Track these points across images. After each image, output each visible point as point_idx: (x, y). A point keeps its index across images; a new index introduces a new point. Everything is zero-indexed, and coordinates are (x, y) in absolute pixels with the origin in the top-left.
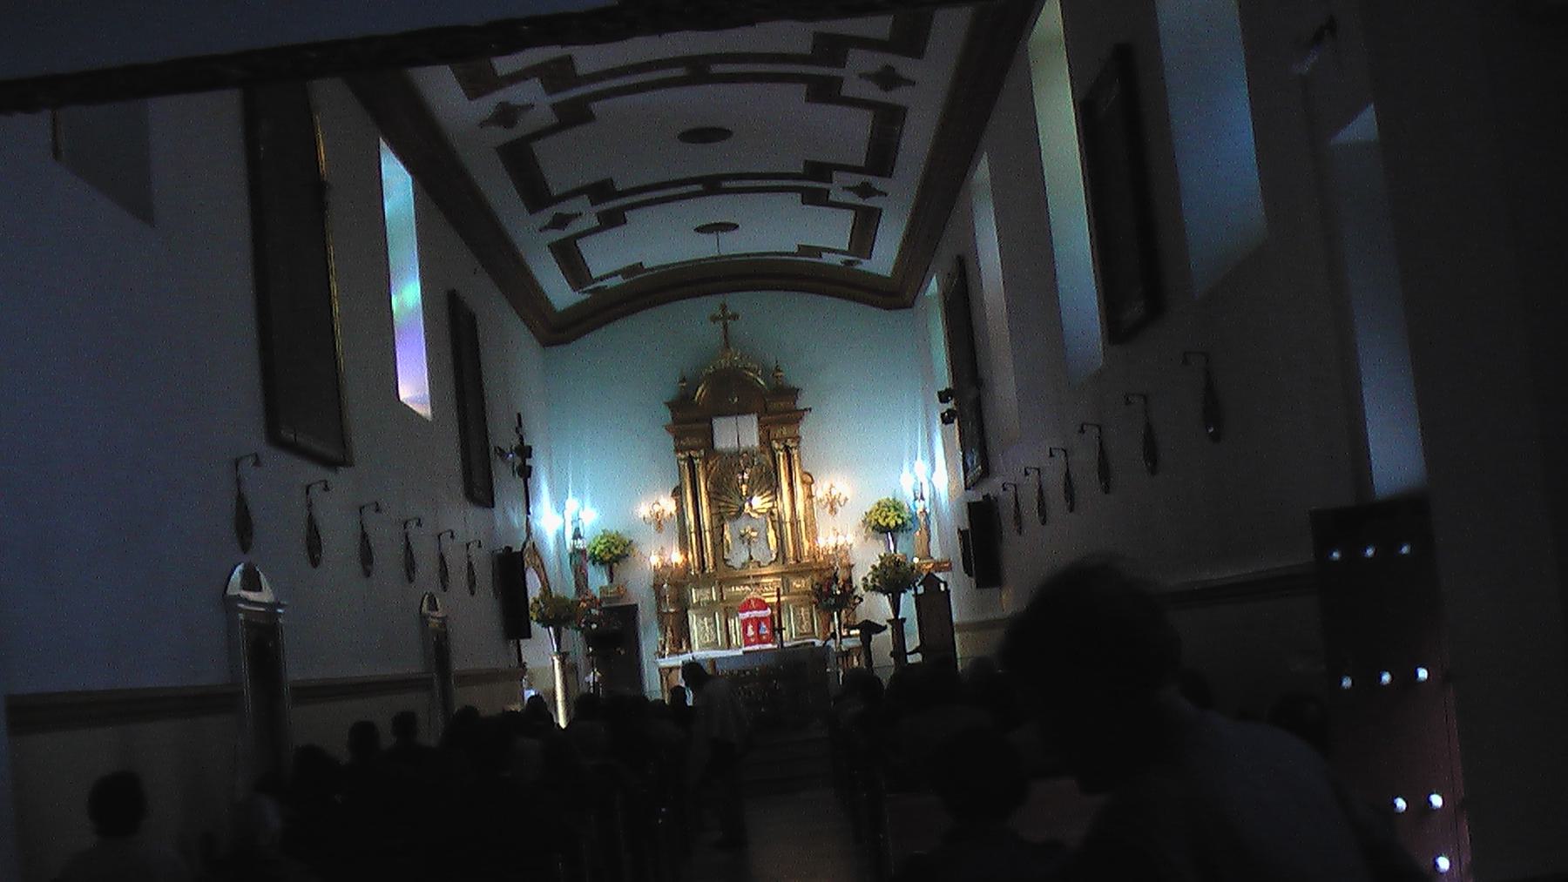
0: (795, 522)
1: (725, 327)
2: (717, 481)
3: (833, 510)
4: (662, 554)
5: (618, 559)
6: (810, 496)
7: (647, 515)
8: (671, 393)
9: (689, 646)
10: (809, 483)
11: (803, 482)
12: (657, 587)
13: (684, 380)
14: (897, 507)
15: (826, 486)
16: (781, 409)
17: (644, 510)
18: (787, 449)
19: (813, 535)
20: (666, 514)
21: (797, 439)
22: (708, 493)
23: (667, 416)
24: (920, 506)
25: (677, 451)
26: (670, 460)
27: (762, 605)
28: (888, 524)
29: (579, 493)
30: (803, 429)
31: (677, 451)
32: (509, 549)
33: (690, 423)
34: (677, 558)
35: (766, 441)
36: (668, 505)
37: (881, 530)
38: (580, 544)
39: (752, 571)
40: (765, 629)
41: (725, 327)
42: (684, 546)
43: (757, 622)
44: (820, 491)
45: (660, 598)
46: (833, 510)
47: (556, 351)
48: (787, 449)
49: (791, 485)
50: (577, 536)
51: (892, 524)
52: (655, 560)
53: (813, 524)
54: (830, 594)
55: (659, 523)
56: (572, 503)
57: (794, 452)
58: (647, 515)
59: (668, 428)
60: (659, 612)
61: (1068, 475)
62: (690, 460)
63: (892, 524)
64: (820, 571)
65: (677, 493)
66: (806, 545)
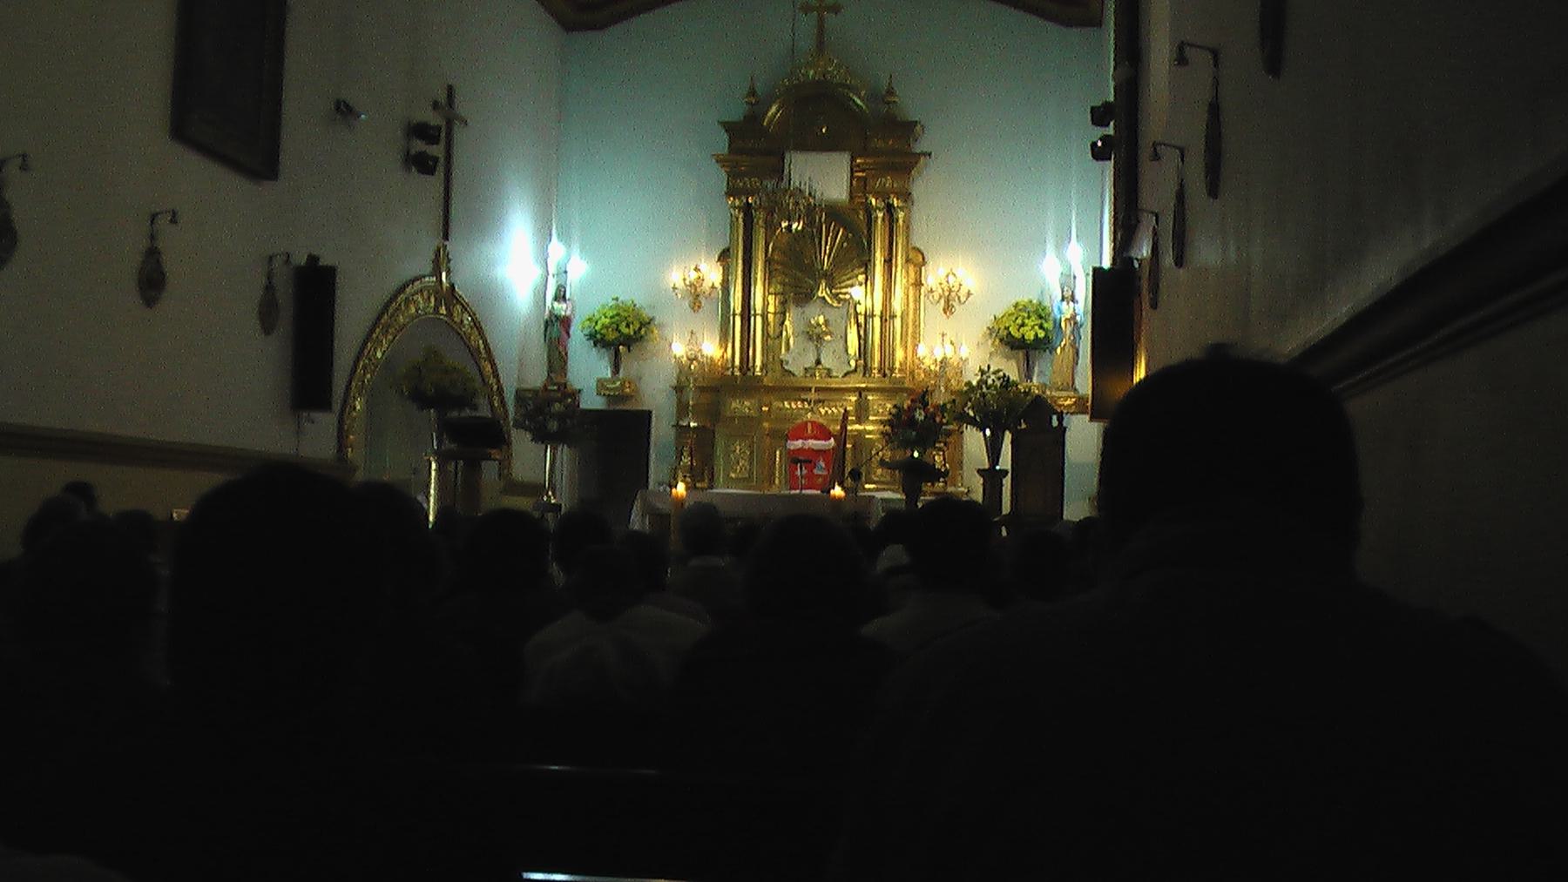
0: (887, 317)
1: (821, 20)
2: (801, 252)
3: (948, 309)
4: (691, 343)
5: (631, 341)
6: (918, 284)
7: (680, 284)
8: (736, 112)
9: (712, 479)
10: (917, 260)
11: (908, 261)
12: (679, 389)
13: (752, 93)
14: (1041, 313)
15: (943, 271)
16: (889, 149)
17: (677, 276)
18: (889, 208)
19: (913, 335)
20: (707, 285)
21: (906, 196)
22: (768, 262)
23: (722, 142)
24: (1067, 310)
25: (729, 194)
26: (725, 209)
27: (823, 433)
28: (1024, 341)
29: (565, 237)
30: (920, 187)
31: (731, 192)
32: (313, 259)
33: (752, 158)
34: (711, 349)
35: (859, 187)
36: (712, 274)
37: (1012, 344)
38: (561, 308)
39: (818, 380)
40: (821, 468)
41: (821, 20)
42: (725, 335)
43: (805, 459)
44: (934, 276)
45: (682, 409)
46: (948, 309)
47: (582, 39)
48: (889, 208)
49: (889, 262)
50: (560, 296)
51: (1030, 336)
52: (679, 349)
53: (917, 326)
54: (912, 422)
55: (695, 296)
56: (556, 249)
57: (901, 215)
58: (680, 284)
59: (720, 160)
60: (677, 426)
61: (1214, 110)
62: (747, 210)
63: (1030, 336)
64: (910, 391)
65: (725, 256)
66: (899, 355)
